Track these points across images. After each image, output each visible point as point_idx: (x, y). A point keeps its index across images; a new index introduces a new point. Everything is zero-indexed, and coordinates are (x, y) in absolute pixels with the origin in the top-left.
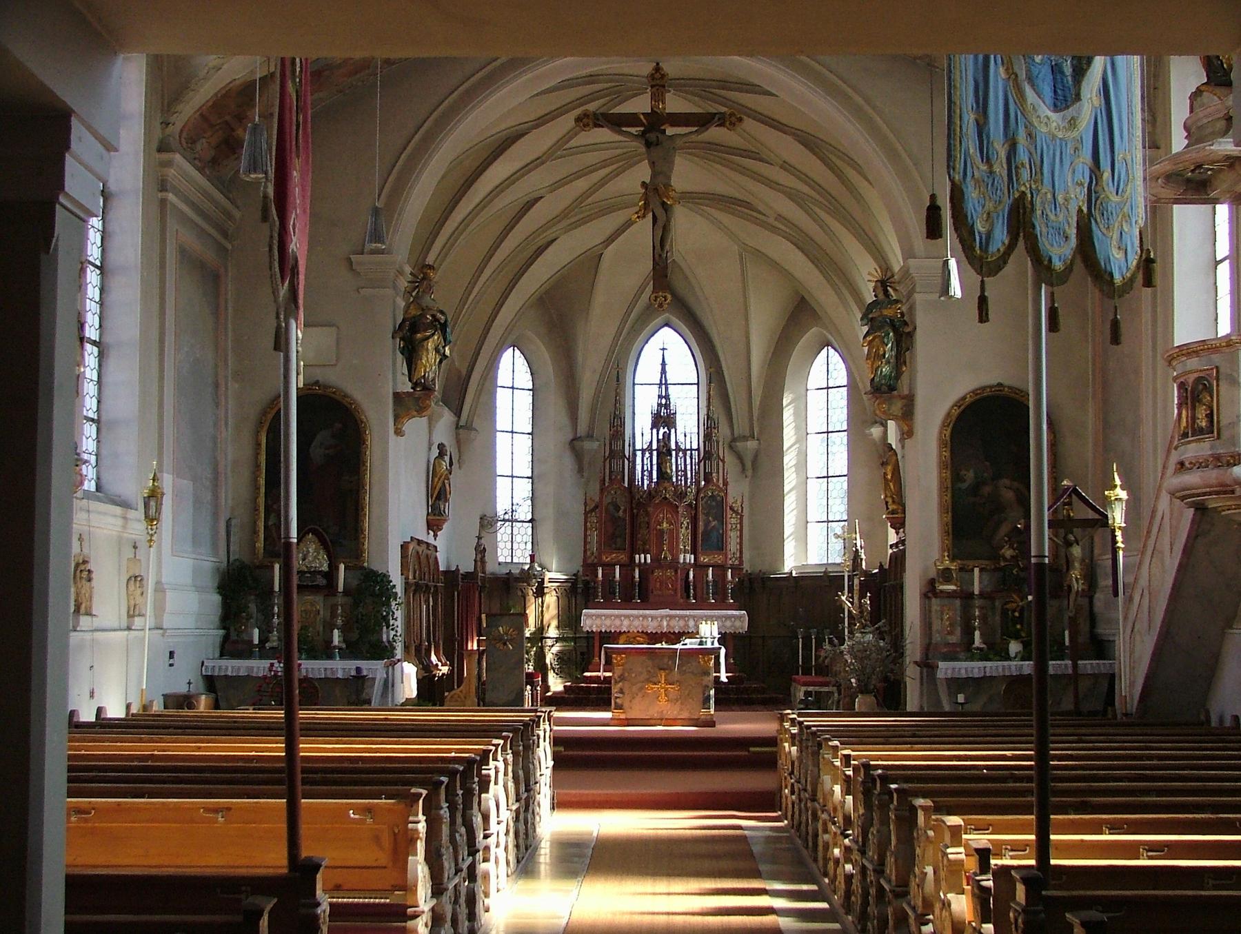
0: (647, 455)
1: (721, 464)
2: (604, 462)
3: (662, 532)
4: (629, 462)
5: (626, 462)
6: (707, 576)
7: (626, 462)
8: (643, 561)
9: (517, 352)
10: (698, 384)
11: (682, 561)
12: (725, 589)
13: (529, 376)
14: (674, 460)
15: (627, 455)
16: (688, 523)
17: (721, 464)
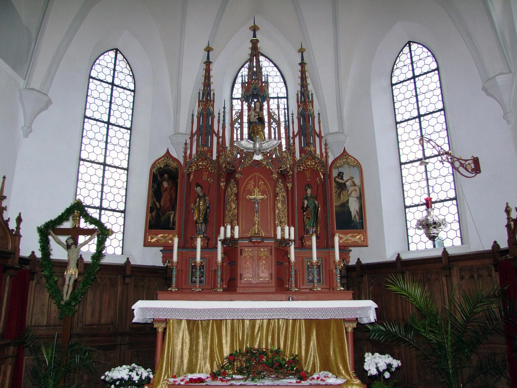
0: (237, 125)
1: (317, 139)
2: (191, 138)
3: (253, 202)
4: (218, 138)
5: (215, 139)
6: (311, 258)
7: (215, 139)
8: (229, 235)
9: (120, 56)
10: (287, 98)
11: (279, 237)
12: (330, 275)
13: (130, 79)
14: (266, 130)
15: (216, 128)
16: (283, 197)
17: (317, 139)
